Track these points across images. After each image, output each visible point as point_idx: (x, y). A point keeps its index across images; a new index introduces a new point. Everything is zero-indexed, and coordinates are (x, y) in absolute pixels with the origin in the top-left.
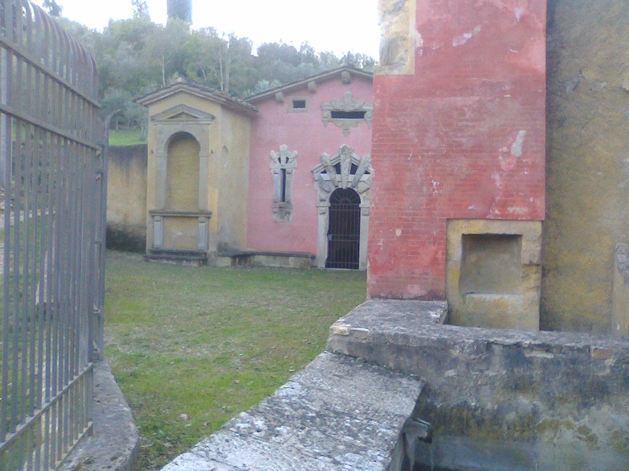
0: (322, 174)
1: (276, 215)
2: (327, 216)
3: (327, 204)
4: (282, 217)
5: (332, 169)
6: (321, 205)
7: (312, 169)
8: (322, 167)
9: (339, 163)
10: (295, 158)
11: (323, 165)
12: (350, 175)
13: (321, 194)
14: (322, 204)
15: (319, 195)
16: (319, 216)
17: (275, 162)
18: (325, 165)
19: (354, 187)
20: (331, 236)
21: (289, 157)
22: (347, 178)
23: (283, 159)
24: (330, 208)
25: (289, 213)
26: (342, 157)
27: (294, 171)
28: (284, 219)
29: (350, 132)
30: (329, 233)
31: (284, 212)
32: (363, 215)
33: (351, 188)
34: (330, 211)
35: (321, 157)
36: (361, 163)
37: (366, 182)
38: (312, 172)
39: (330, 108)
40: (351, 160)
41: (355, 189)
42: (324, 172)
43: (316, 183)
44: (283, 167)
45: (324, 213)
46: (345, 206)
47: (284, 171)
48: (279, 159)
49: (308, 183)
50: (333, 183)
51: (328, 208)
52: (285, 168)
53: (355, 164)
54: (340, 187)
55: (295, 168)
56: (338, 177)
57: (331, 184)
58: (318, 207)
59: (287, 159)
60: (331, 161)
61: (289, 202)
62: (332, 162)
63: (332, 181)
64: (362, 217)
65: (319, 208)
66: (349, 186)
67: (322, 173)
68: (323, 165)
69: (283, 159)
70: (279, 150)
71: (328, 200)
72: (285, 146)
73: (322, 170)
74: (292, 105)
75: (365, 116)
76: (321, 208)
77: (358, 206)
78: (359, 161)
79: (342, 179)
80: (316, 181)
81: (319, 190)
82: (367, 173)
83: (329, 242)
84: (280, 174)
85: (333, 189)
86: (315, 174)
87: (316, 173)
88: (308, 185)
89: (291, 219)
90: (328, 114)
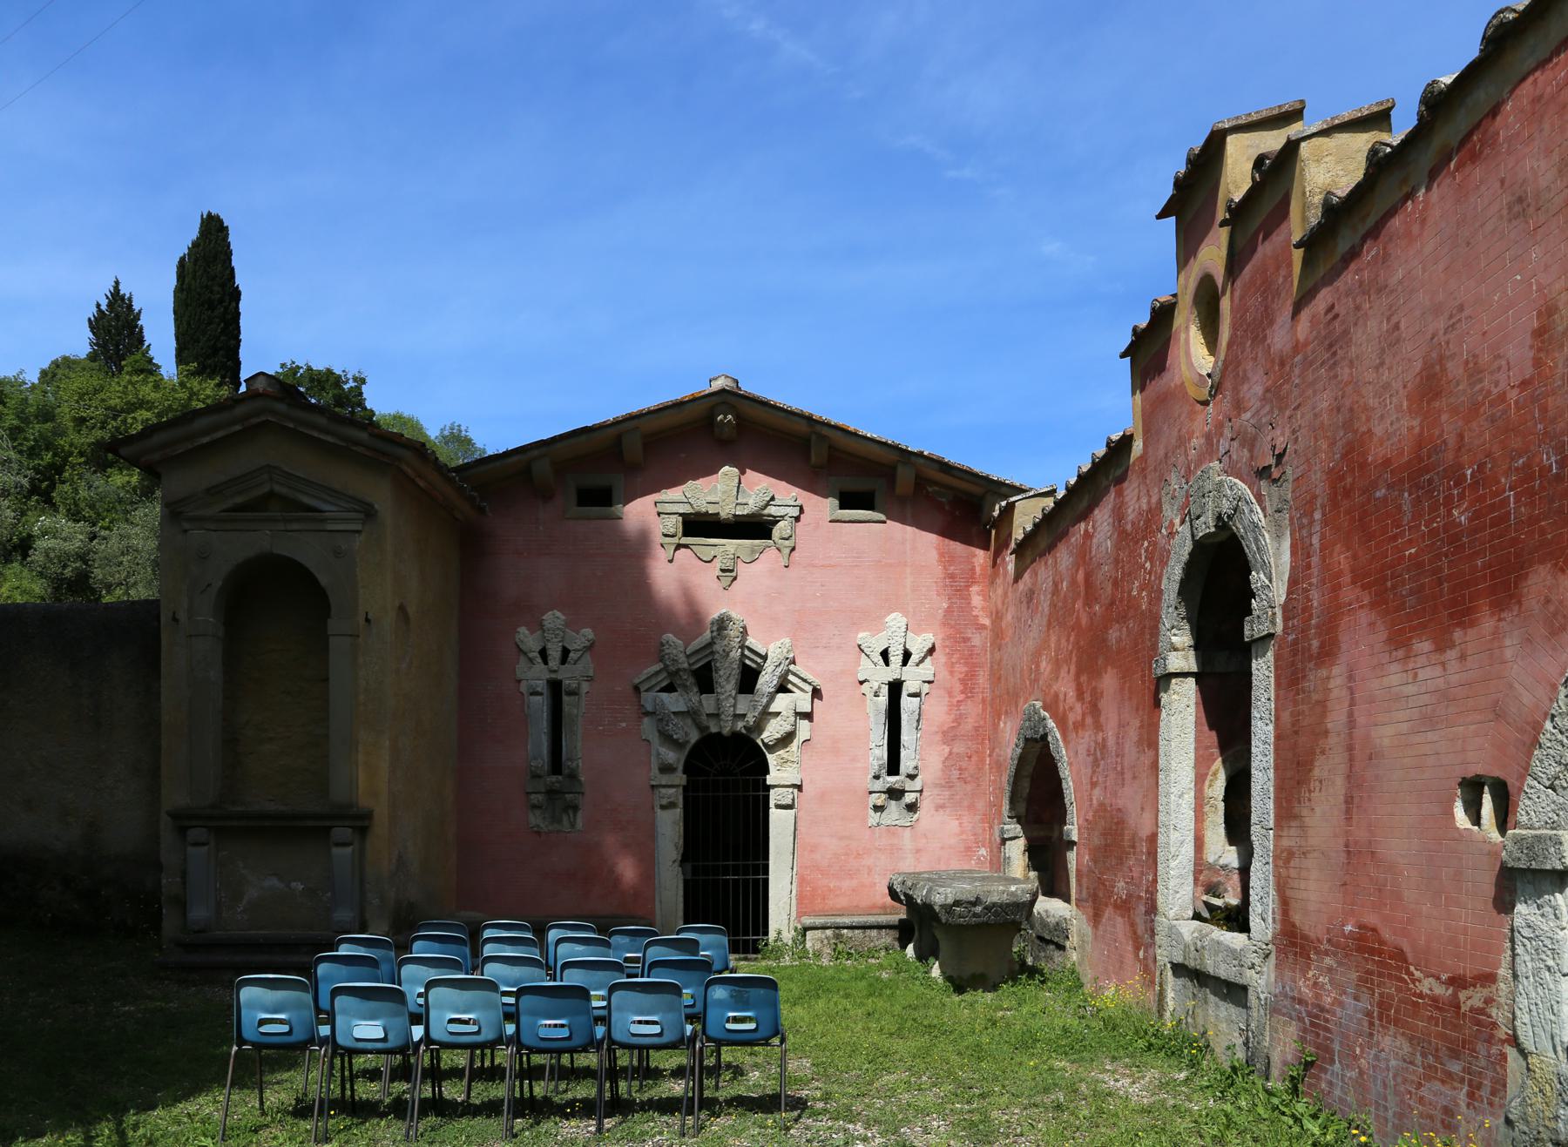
0: (664, 695)
2: (678, 812)
3: (680, 778)
5: (691, 681)
6: (664, 783)
7: (637, 681)
8: (664, 675)
9: (709, 663)
11: (666, 666)
12: (741, 697)
13: (663, 750)
14: (665, 779)
15: (659, 754)
16: (658, 811)
18: (672, 668)
20: (689, 866)
22: (734, 706)
24: (685, 789)
28: (560, 821)
30: (685, 859)
32: (778, 806)
33: (744, 731)
34: (685, 798)
35: (663, 645)
37: (784, 713)
38: (637, 689)
40: (743, 654)
42: (670, 688)
45: (672, 805)
47: (555, 687)
49: (625, 721)
50: (694, 720)
51: (681, 790)
52: (560, 677)
53: (754, 666)
54: (714, 729)
56: (708, 703)
57: (689, 721)
58: (653, 786)
60: (688, 657)
62: (691, 662)
63: (692, 714)
64: (774, 813)
65: (656, 791)
67: (663, 690)
68: (666, 666)
71: (681, 768)
76: (663, 791)
78: (765, 658)
80: (647, 714)
81: (654, 738)
82: (783, 688)
83: (686, 882)
84: (545, 697)
85: (694, 736)
86: (644, 695)
87: (647, 691)
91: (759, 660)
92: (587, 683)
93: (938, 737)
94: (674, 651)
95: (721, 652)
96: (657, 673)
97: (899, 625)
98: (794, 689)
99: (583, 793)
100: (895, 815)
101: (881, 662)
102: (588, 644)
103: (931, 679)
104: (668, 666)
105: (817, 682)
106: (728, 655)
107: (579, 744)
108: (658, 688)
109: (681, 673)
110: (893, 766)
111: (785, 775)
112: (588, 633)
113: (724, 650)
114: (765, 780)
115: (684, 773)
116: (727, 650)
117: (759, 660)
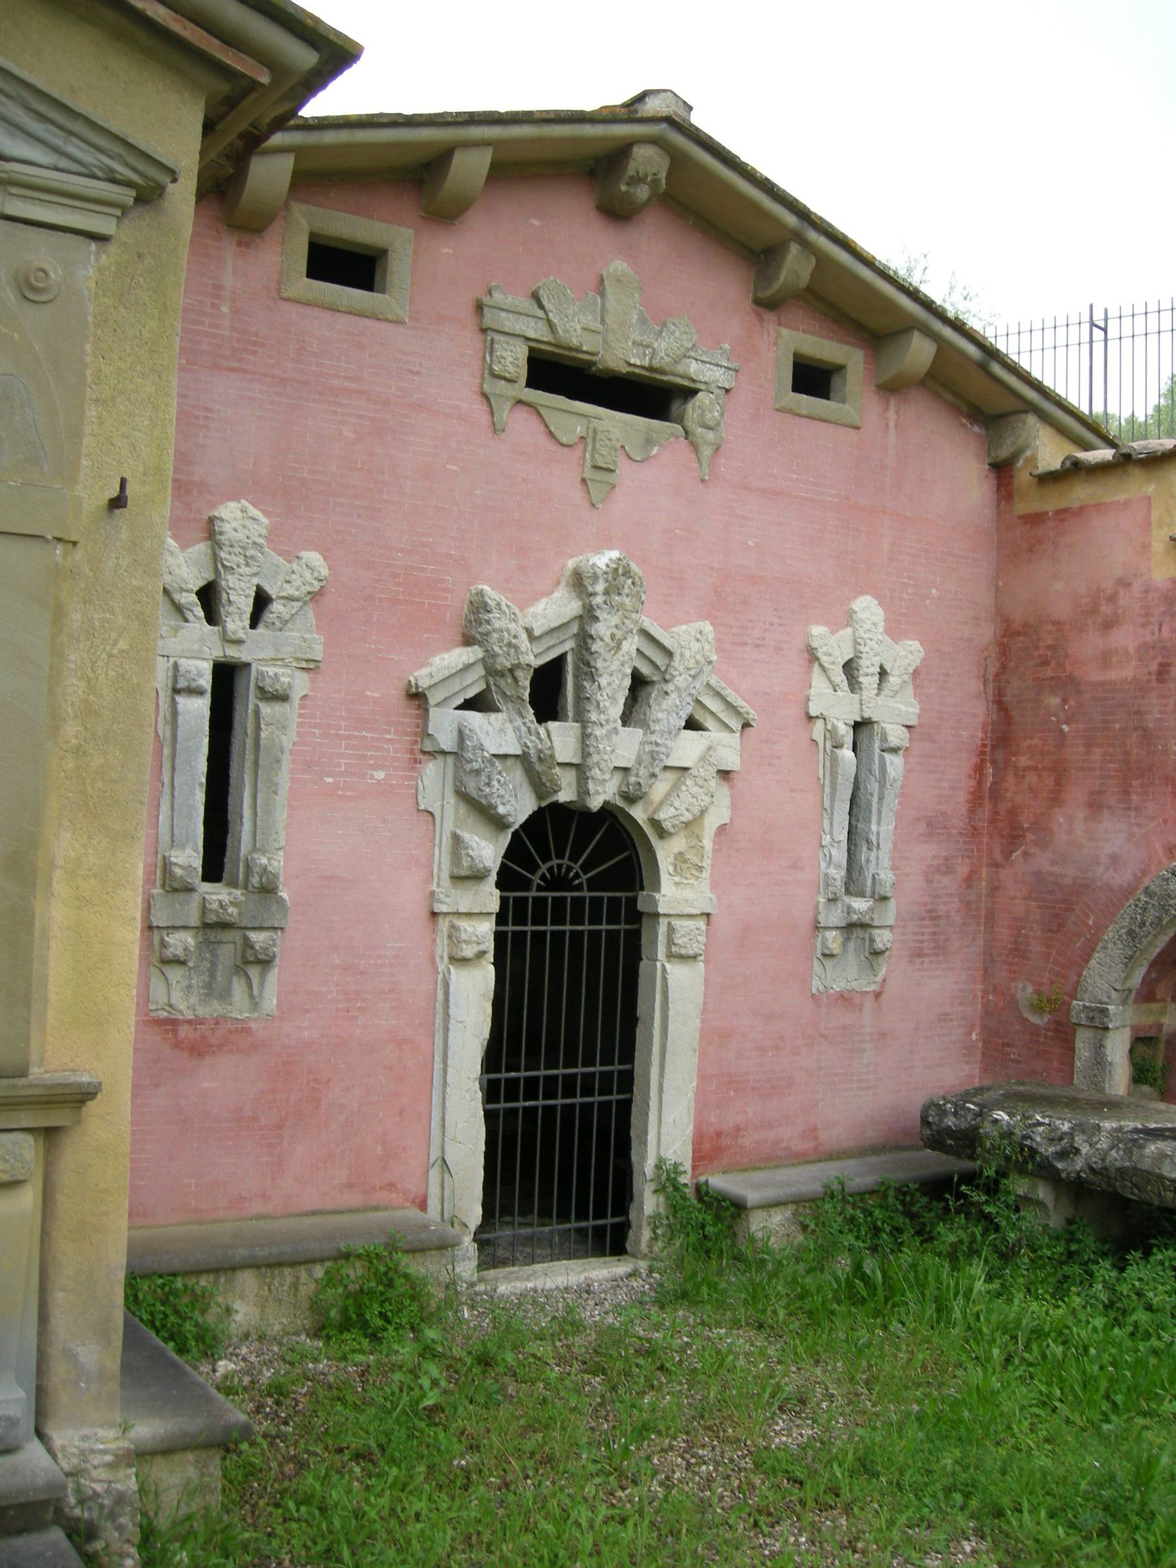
1: (175, 974)
3: (489, 897)
4: (215, 991)
6: (462, 909)
8: (480, 671)
10: (315, 597)
17: (179, 609)
18: (504, 662)
19: (631, 799)
21: (272, 591)
23: (240, 602)
25: (265, 963)
26: (603, 628)
27: (300, 685)
29: (614, 487)
31: (227, 953)
33: (620, 803)
36: (676, 663)
39: (535, 330)
41: (638, 813)
43: (431, 770)
44: (234, 653)
46: (559, 903)
48: (209, 596)
54: (565, 795)
55: (311, 667)
59: (262, 601)
61: (268, 890)
66: (604, 791)
69: (240, 602)
70: (211, 531)
72: (254, 512)
73: (470, 694)
74: (302, 264)
75: (692, 410)
77: (632, 902)
79: (585, 754)
81: (450, 813)
82: (692, 724)
88: (380, 775)
89: (271, 1001)
90: (514, 359)
91: (660, 660)
92: (305, 676)
93: (922, 828)
94: (512, 626)
95: (608, 639)
96: (467, 667)
97: (874, 619)
98: (709, 723)
99: (282, 929)
100: (853, 972)
101: (845, 685)
102: (317, 586)
103: (913, 722)
104: (494, 656)
105: (752, 715)
106: (619, 647)
107: (281, 815)
108: (460, 701)
109: (519, 674)
110: (853, 881)
111: (687, 893)
112: (313, 557)
113: (613, 636)
114: (635, 900)
115: (499, 885)
116: (619, 634)
117: (660, 660)
